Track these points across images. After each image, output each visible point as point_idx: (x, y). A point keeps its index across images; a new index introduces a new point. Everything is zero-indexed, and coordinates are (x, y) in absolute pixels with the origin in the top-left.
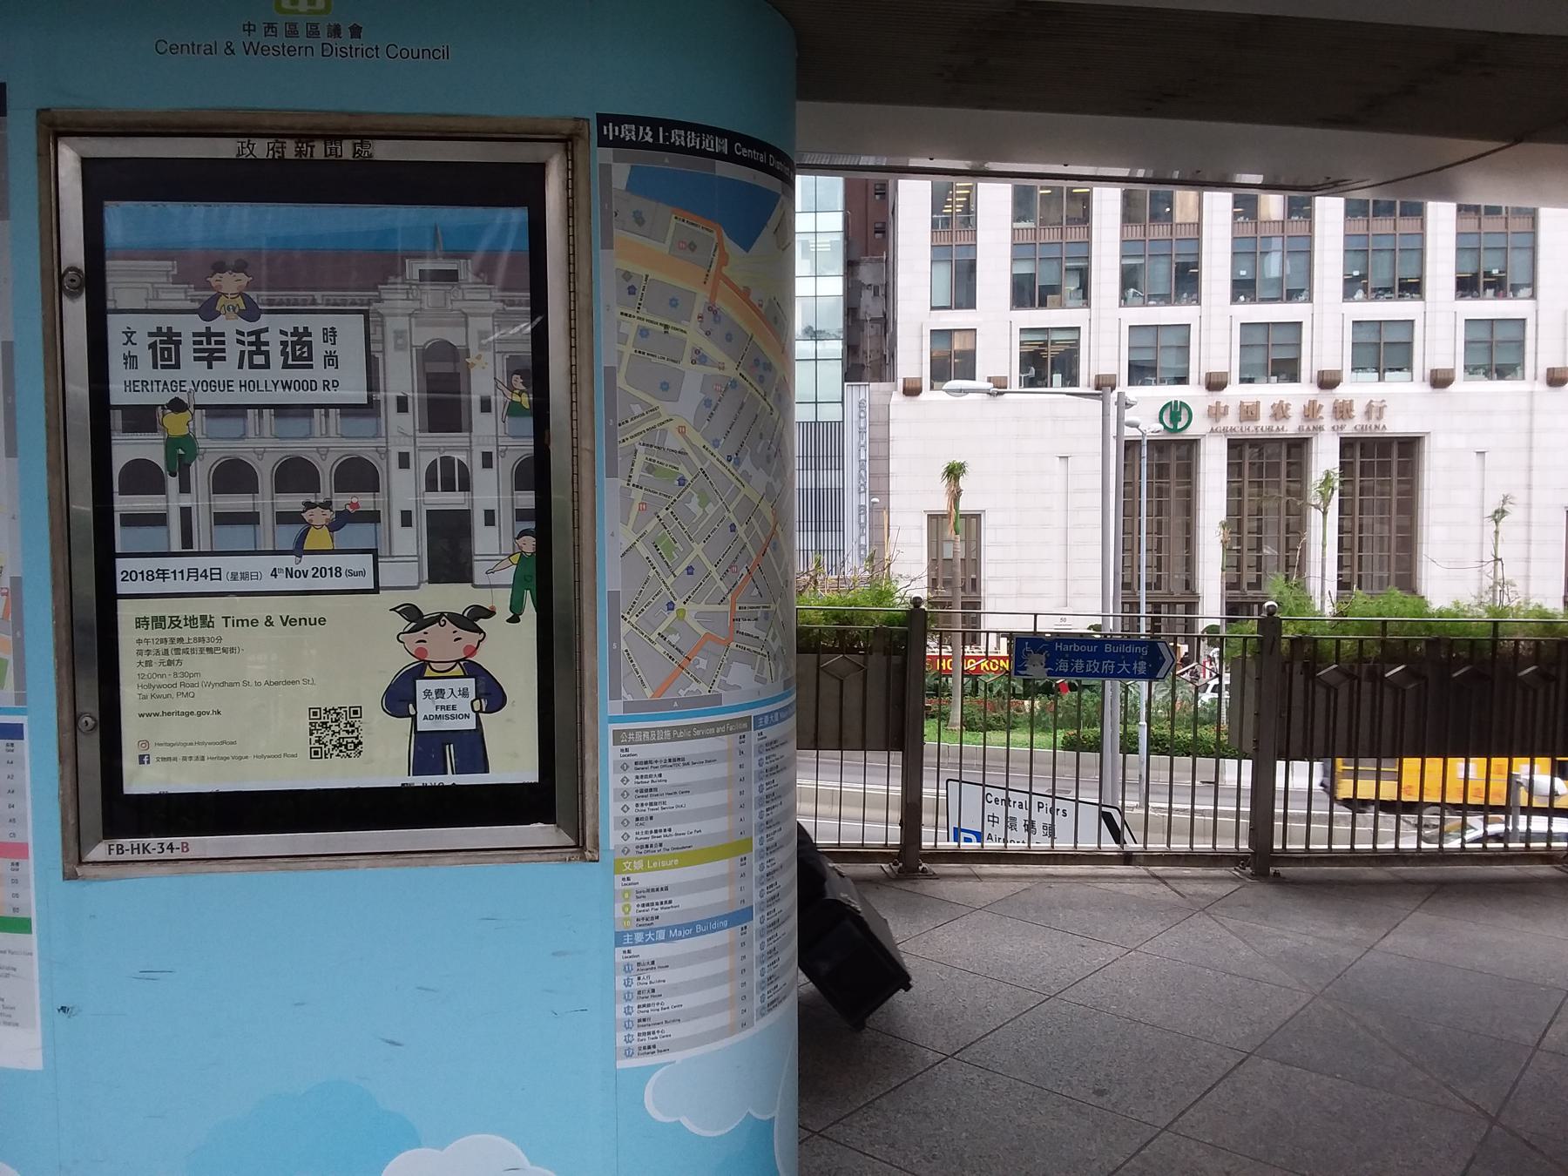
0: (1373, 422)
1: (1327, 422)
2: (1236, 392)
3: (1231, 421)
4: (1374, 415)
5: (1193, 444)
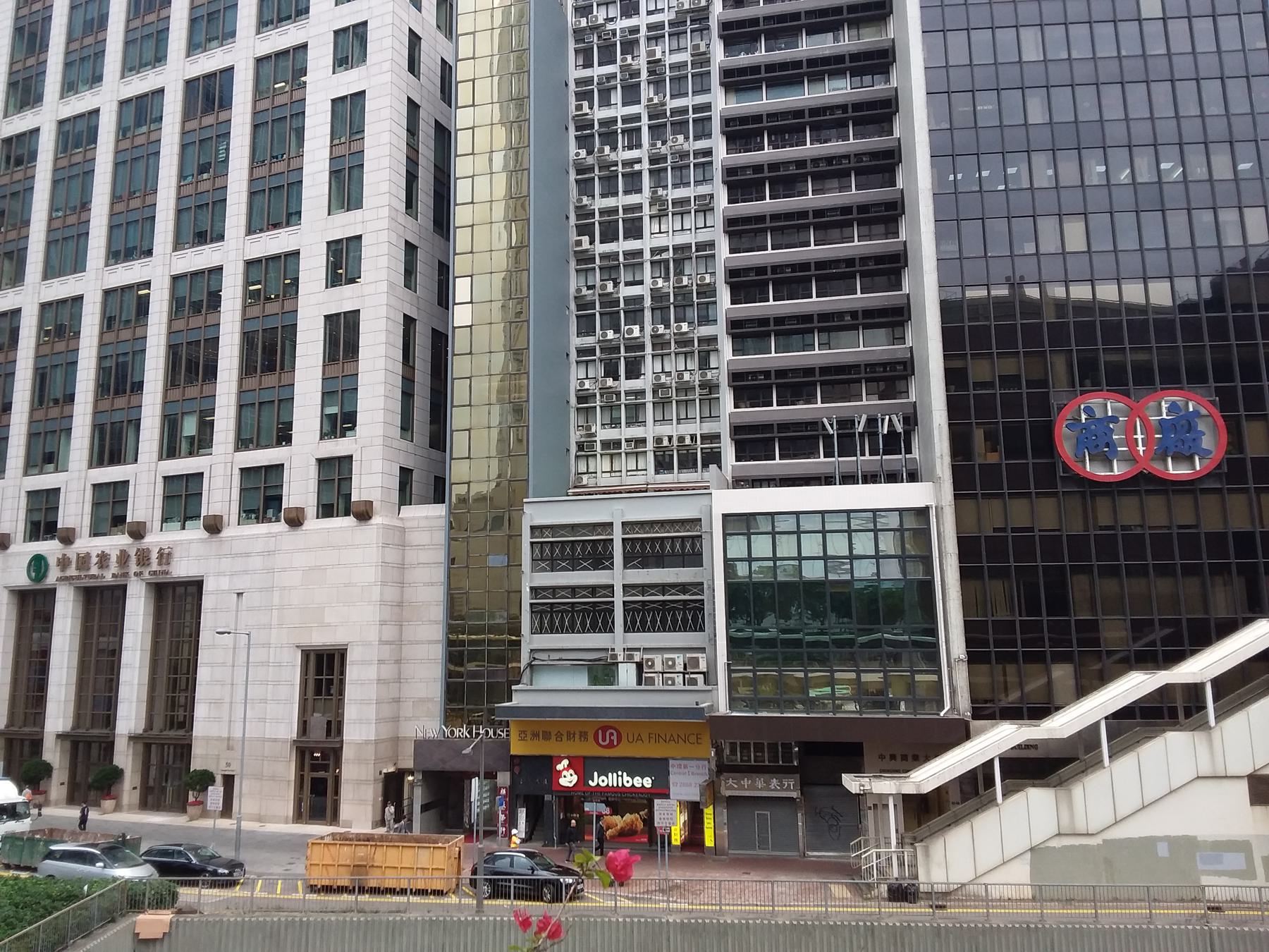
0: (164, 568)
1: (133, 567)
4: (164, 561)
5: (52, 592)
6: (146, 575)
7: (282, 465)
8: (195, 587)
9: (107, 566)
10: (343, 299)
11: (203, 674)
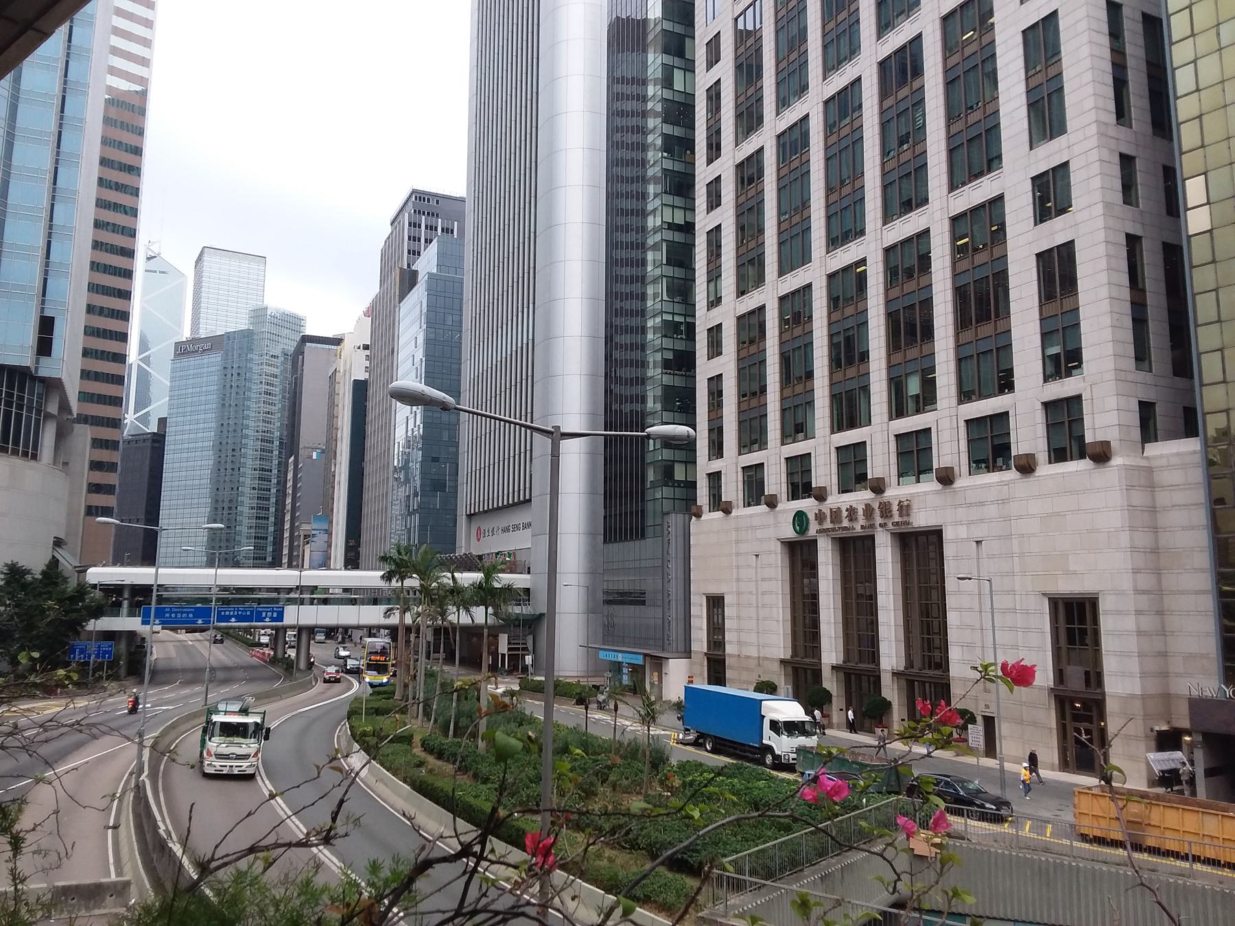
0: (905, 519)
1: (878, 520)
2: (836, 500)
3: (828, 524)
5: (814, 542)
6: (890, 526)
7: (1007, 413)
8: (935, 536)
9: (856, 519)
10: (1056, 232)
11: (952, 618)
